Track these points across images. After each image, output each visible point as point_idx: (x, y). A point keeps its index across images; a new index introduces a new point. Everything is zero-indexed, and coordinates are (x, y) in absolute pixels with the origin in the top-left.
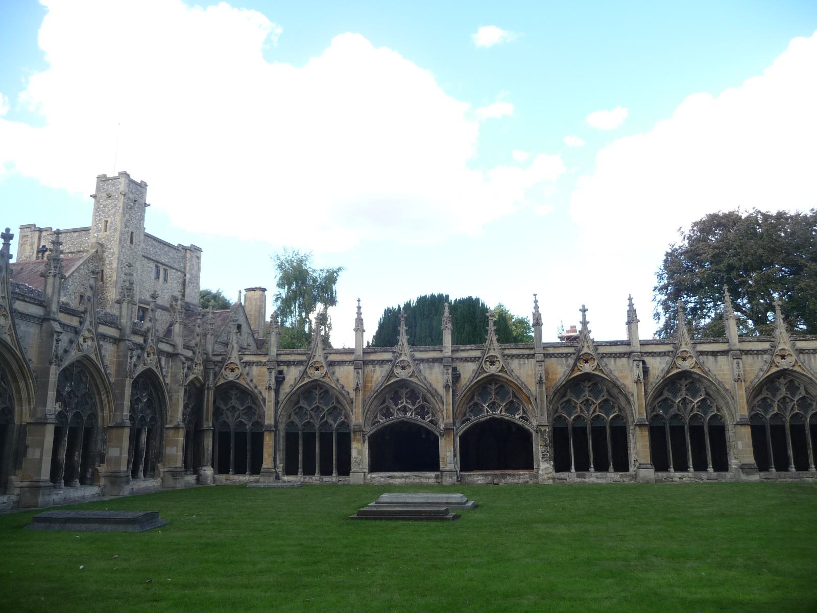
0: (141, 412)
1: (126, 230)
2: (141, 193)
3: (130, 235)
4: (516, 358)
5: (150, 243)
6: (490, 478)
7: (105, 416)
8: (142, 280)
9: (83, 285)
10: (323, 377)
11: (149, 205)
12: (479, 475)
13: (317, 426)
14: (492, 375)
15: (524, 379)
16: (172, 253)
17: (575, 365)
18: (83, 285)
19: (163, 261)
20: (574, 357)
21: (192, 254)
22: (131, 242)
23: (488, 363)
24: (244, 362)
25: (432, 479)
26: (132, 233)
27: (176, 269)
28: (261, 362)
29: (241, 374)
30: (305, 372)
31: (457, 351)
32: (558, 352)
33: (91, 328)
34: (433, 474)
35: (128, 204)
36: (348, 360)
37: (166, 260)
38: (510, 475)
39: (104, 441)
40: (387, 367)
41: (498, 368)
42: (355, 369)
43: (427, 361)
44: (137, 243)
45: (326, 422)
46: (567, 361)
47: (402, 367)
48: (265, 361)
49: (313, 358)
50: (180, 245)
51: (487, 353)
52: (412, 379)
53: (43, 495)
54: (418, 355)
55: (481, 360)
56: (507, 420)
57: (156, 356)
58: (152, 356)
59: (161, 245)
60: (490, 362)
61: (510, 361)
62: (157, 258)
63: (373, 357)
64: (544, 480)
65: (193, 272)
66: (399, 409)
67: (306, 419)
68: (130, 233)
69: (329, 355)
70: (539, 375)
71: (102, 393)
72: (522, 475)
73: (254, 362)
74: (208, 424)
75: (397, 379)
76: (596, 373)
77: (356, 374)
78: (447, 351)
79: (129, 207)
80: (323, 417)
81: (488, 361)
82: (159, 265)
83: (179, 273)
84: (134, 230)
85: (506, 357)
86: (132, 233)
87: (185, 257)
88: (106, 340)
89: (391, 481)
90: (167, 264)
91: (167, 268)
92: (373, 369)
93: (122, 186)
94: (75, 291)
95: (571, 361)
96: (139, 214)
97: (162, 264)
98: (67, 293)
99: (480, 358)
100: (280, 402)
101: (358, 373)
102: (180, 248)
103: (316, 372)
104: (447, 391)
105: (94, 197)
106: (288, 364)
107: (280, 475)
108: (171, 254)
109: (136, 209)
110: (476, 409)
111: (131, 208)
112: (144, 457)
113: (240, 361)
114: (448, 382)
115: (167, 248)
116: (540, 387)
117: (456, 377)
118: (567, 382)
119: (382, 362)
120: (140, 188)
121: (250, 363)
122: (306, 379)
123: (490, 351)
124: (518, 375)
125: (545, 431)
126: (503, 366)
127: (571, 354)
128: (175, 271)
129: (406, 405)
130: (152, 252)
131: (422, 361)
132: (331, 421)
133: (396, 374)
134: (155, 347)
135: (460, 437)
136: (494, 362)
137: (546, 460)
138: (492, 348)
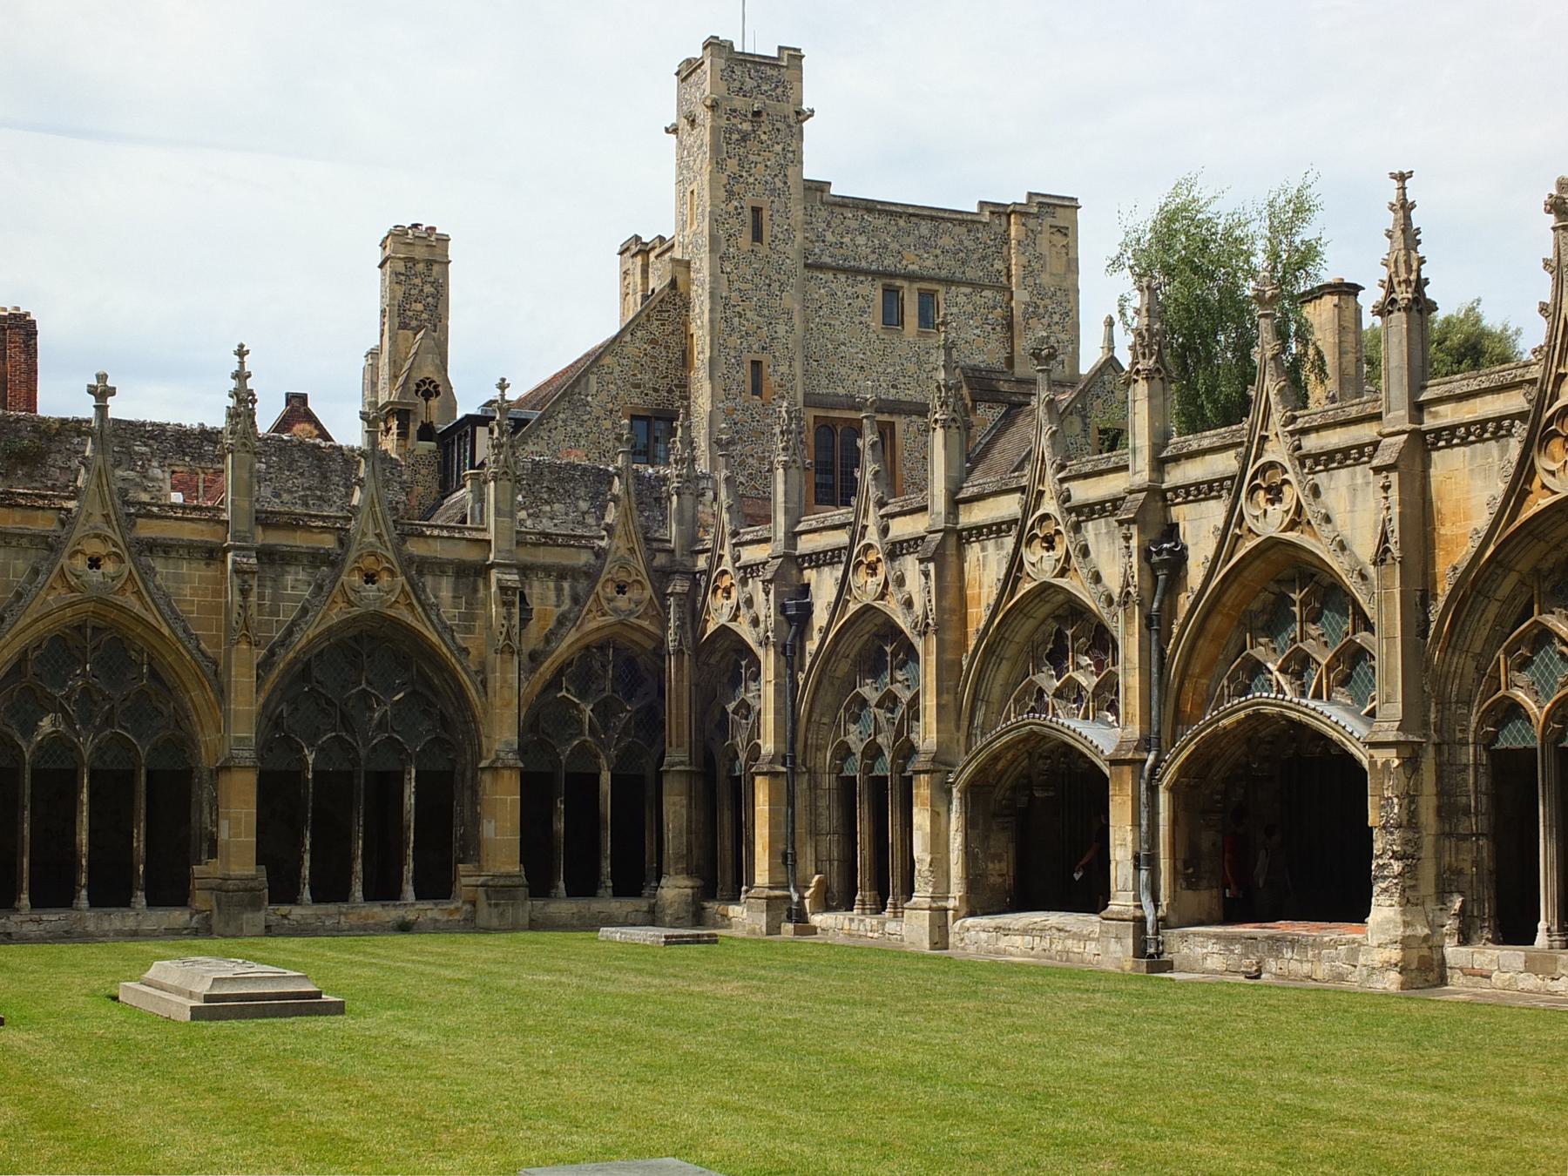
0: (382, 725)
1: (731, 208)
3: (749, 221)
4: (1342, 465)
5: (854, 224)
7: (210, 744)
8: (832, 341)
9: (637, 386)
10: (882, 596)
12: (1208, 936)
14: (1272, 543)
18: (637, 386)
19: (915, 267)
20: (1520, 430)
21: (1032, 223)
22: (757, 236)
23: (1261, 496)
24: (739, 568)
26: (756, 211)
27: (970, 284)
30: (843, 586)
31: (1176, 459)
32: (1468, 417)
33: (110, 532)
37: (929, 263)
38: (1293, 943)
39: (214, 804)
40: (1009, 542)
44: (780, 236)
46: (1504, 451)
49: (863, 536)
50: (982, 204)
51: (1257, 458)
57: (401, 579)
58: (385, 579)
59: (902, 223)
60: (1268, 490)
61: (1321, 479)
65: (1045, 279)
68: (748, 213)
71: (189, 685)
79: (735, 136)
82: (898, 283)
83: (987, 293)
84: (764, 201)
85: (1308, 462)
86: (756, 211)
88: (173, 554)
91: (936, 287)
92: (981, 555)
93: (705, 83)
94: (610, 406)
96: (778, 148)
97: (911, 277)
98: (585, 418)
100: (801, 683)
101: (926, 575)
102: (986, 217)
103: (870, 580)
105: (674, 130)
106: (819, 560)
108: (946, 241)
109: (764, 137)
111: (744, 138)
112: (411, 845)
113: (735, 563)
115: (925, 228)
119: (996, 529)
120: (770, 72)
122: (850, 604)
123: (1268, 446)
124: (1346, 533)
125: (1386, 764)
127: (1512, 417)
128: (968, 290)
130: (864, 251)
134: (391, 555)
135: (1173, 789)
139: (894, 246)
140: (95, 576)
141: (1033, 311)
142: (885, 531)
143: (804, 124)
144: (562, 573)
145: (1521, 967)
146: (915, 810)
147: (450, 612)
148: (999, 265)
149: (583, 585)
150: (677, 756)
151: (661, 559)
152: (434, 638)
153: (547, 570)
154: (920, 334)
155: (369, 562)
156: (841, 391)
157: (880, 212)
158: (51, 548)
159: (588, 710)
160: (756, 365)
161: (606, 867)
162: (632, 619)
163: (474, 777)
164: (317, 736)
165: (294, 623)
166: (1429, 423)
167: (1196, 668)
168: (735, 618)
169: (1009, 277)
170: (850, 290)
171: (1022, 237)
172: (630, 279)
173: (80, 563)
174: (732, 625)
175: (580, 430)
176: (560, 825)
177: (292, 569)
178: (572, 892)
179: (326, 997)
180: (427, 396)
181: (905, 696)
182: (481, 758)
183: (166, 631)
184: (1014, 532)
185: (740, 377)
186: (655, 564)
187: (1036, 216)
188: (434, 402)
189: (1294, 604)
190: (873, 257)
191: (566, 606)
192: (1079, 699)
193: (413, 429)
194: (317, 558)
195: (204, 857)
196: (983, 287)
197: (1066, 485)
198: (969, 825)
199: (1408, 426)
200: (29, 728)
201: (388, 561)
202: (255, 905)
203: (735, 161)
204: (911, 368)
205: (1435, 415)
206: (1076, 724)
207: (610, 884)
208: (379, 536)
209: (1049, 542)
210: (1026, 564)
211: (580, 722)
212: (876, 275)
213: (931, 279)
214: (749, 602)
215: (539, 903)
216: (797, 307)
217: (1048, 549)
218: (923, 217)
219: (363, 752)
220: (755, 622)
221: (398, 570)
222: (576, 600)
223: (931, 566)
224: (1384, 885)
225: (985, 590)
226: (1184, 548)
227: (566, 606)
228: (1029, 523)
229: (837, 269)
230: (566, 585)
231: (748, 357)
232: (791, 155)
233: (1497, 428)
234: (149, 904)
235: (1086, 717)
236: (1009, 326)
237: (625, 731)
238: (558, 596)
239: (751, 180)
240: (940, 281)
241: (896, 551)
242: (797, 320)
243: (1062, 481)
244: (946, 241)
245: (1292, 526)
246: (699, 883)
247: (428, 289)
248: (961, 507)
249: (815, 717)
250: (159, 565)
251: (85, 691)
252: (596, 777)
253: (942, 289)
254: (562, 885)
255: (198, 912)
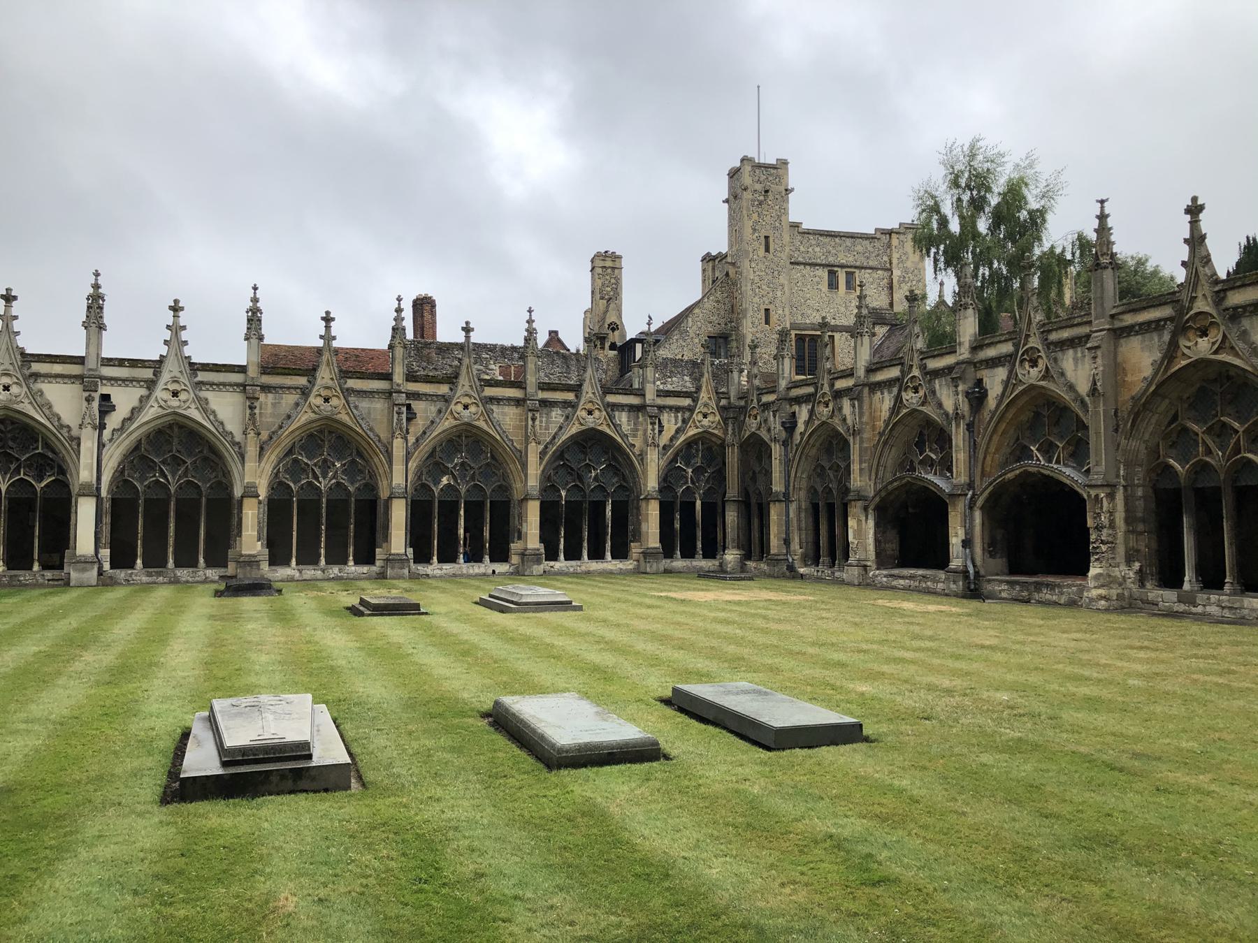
0: (596, 479)
1: (754, 237)
2: (778, 176)
5: (814, 242)
8: (803, 298)
9: (711, 322)
10: (831, 417)
11: (792, 190)
16: (860, 246)
17: (1173, 347)
18: (711, 322)
20: (1170, 326)
21: (902, 237)
22: (767, 250)
23: (1027, 365)
26: (767, 238)
27: (871, 268)
30: (812, 412)
35: (753, 201)
37: (851, 259)
40: (895, 390)
46: (1160, 337)
50: (876, 230)
53: (392, 568)
57: (604, 413)
58: (597, 413)
60: (1030, 361)
62: (831, 260)
64: (1091, 600)
65: (909, 264)
68: (763, 239)
70: (1091, 379)
74: (732, 492)
76: (1222, 357)
78: (963, 350)
79: (756, 203)
82: (836, 269)
83: (879, 272)
84: (770, 234)
86: (767, 238)
87: (889, 246)
90: (852, 264)
95: (1167, 337)
97: (842, 266)
99: (1011, 356)
102: (878, 235)
105: (727, 201)
107: (797, 564)
108: (859, 248)
110: (1022, 453)
111: (761, 203)
114: (957, 409)
115: (848, 242)
117: (977, 397)
118: (1159, 386)
119: (889, 383)
120: (772, 171)
123: (1030, 339)
127: (1166, 320)
128: (870, 271)
139: (834, 252)
140: (466, 413)
141: (903, 280)
142: (832, 385)
143: (790, 195)
144: (678, 409)
146: (849, 519)
147: (626, 428)
148: (886, 258)
149: (687, 415)
150: (732, 492)
151: (723, 402)
152: (619, 440)
153: (671, 408)
154: (846, 293)
155: (589, 406)
156: (808, 321)
157: (827, 236)
158: (446, 401)
159: (690, 471)
160: (767, 310)
161: (699, 545)
162: (710, 430)
163: (638, 503)
164: (567, 484)
165: (556, 434)
166: (1118, 324)
167: (992, 449)
168: (759, 429)
169: (891, 263)
170: (812, 274)
171: (897, 244)
172: (707, 273)
173: (460, 408)
174: (758, 432)
175: (684, 344)
176: (677, 526)
177: (555, 409)
178: (684, 556)
179: (573, 604)
180: (613, 330)
181: (843, 465)
182: (641, 494)
183: (498, 437)
184: (897, 385)
185: (759, 316)
186: (721, 404)
187: (904, 234)
188: (616, 333)
189: (1044, 417)
190: (823, 257)
191: (679, 424)
192: (931, 466)
193: (607, 345)
194: (566, 404)
195: (516, 540)
196: (877, 269)
197: (924, 362)
198: (877, 525)
199: (1107, 327)
200: (437, 482)
201: (598, 405)
202: (539, 562)
203: (756, 214)
204: (843, 309)
205: (1121, 320)
206: (930, 477)
207: (701, 552)
208: (594, 393)
209: (916, 390)
210: (904, 401)
211: (687, 478)
212: (824, 266)
213: (851, 267)
214: (766, 421)
215: (668, 561)
216: (786, 282)
217: (915, 393)
218: (848, 237)
219: (587, 492)
220: (769, 430)
221: (603, 409)
222: (684, 421)
225: (883, 413)
226: (986, 391)
227: (679, 424)
228: (905, 380)
229: (805, 264)
230: (679, 415)
231: (763, 307)
232: (783, 211)
234: (491, 561)
235: (935, 474)
236: (891, 288)
237: (707, 481)
238: (676, 420)
239: (764, 223)
240: (856, 267)
241: (838, 395)
242: (786, 289)
243: (922, 359)
244: (859, 248)
245: (1044, 378)
246: (743, 552)
247: (613, 281)
249: (798, 475)
250: (494, 408)
251: (463, 464)
252: (694, 503)
253: (857, 271)
254: (679, 553)
255: (513, 565)
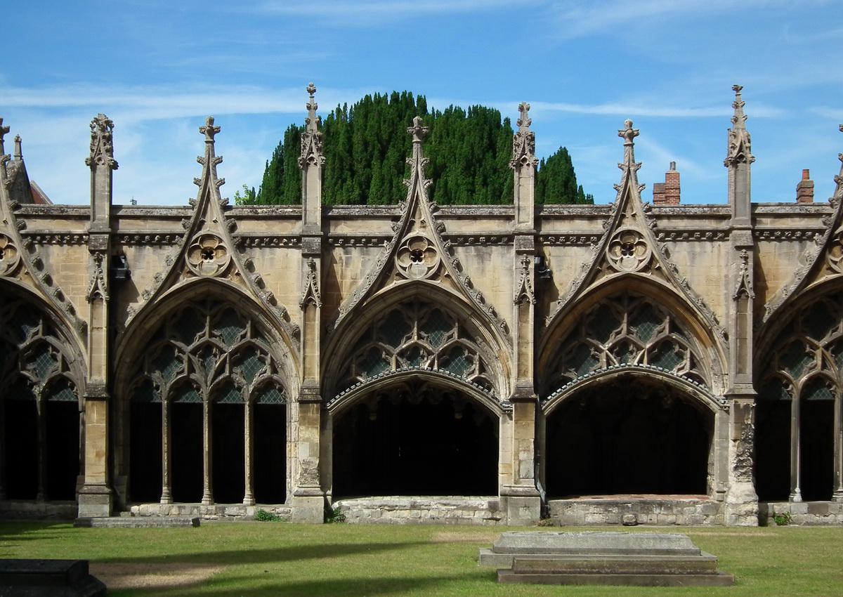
4: (686, 240)
6: (615, 510)
10: (224, 275)
12: (590, 504)
13: (205, 391)
14: (628, 277)
15: (699, 287)
17: (822, 258)
23: (618, 249)
25: (483, 513)
28: (72, 235)
29: (21, 264)
31: (548, 218)
34: (483, 501)
36: (285, 233)
38: (660, 505)
41: (641, 261)
42: (304, 256)
43: (475, 240)
45: (229, 383)
46: (802, 249)
47: (414, 253)
48: (80, 231)
49: (200, 229)
52: (436, 283)
54: (453, 227)
55: (601, 243)
56: (661, 381)
60: (623, 246)
61: (670, 245)
63: (343, 229)
66: (401, 354)
67: (178, 373)
69: (238, 223)
70: (740, 279)
72: (688, 505)
73: (52, 236)
75: (403, 282)
77: (307, 269)
78: (523, 217)
80: (221, 370)
81: (618, 243)
85: (661, 235)
89: (388, 516)
92: (344, 257)
95: (813, 250)
99: (599, 237)
101: (313, 266)
104: (522, 313)
113: (19, 230)
116: (738, 306)
121: (43, 236)
123: (625, 221)
124: (688, 278)
125: (747, 406)
126: (653, 258)
127: (814, 231)
129: (420, 342)
131: (464, 240)
132: (238, 378)
133: (402, 271)
136: (631, 246)
137: (744, 473)
138: (628, 213)
142: (233, 228)
145: (806, 511)
223: (318, 262)
224: (743, 471)
233: (804, 236)
241: (243, 244)
248: (332, 222)
